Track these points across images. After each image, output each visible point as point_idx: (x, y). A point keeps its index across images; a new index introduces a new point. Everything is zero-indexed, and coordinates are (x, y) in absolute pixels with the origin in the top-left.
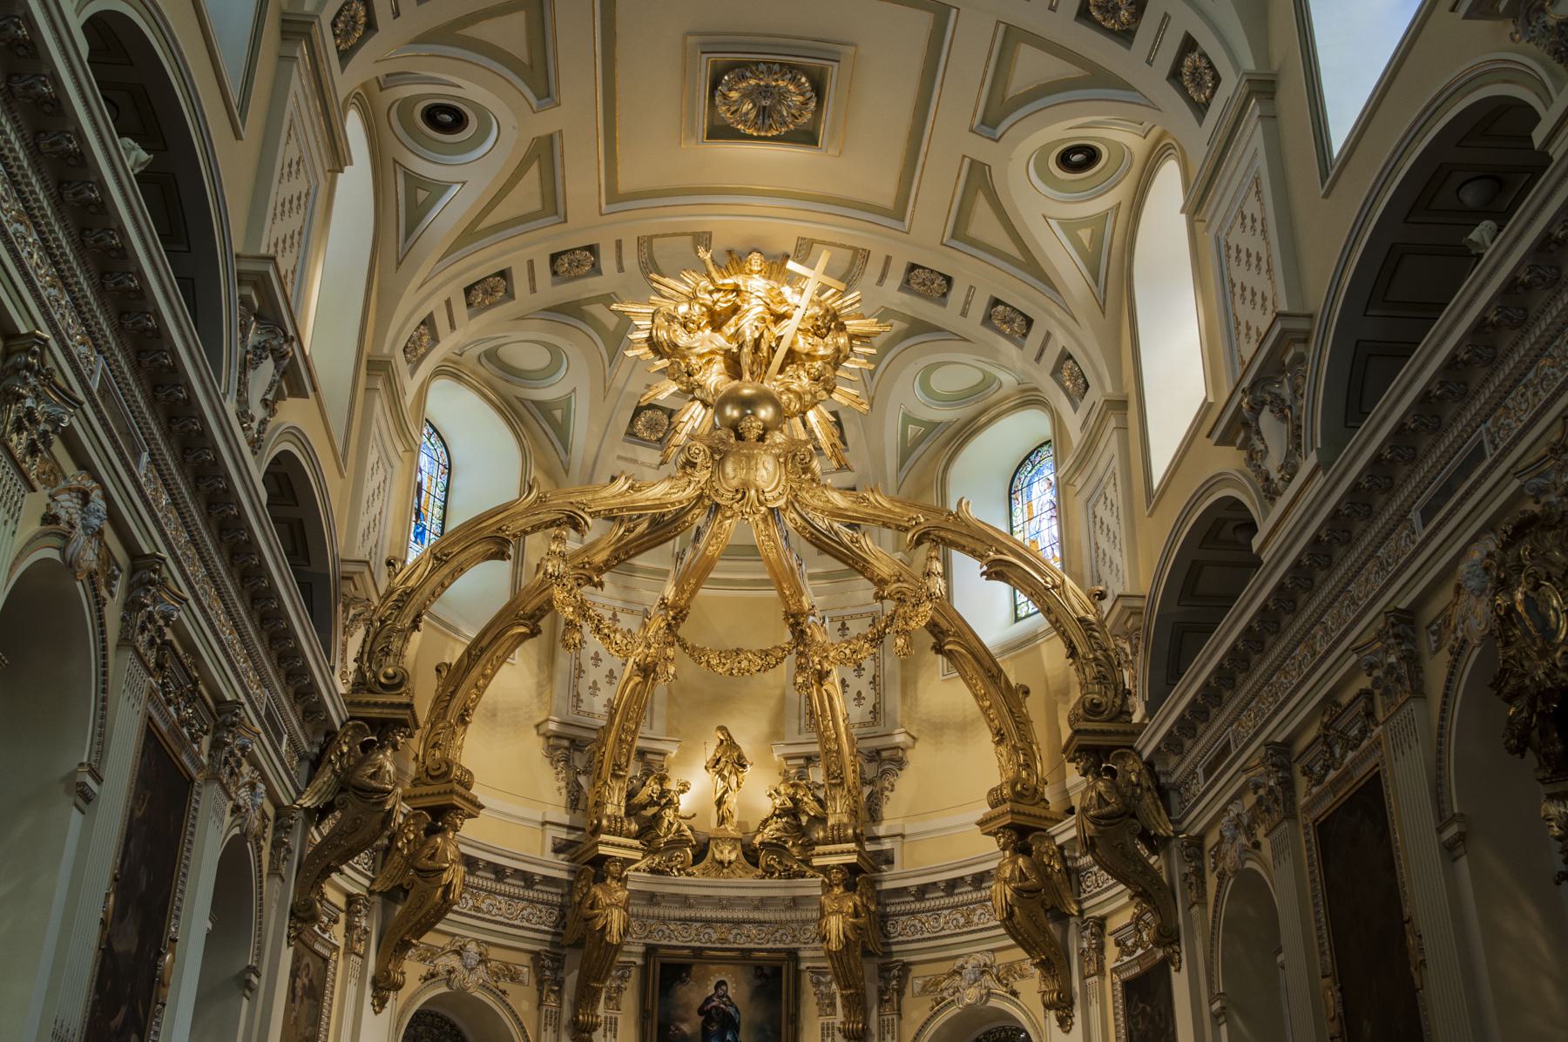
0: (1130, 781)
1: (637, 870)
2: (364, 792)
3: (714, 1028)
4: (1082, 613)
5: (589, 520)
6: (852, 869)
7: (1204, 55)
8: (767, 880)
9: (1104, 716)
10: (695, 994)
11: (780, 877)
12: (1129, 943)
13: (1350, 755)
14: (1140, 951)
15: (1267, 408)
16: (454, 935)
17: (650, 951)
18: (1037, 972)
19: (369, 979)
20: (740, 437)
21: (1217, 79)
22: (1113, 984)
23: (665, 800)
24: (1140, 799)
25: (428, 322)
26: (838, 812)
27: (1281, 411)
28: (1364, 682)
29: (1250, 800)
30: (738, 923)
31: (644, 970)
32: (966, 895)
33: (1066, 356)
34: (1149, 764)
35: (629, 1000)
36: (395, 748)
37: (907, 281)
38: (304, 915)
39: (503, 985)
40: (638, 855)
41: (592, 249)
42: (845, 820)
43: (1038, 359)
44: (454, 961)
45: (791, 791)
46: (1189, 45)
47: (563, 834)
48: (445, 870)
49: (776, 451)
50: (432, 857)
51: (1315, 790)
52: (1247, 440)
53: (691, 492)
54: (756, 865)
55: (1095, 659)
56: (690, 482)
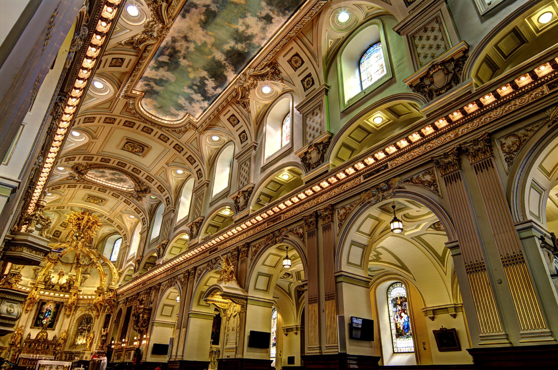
3: (47, 312)
6: (75, 293)
10: (46, 307)
23: (50, 279)
31: (39, 303)
40: (43, 288)
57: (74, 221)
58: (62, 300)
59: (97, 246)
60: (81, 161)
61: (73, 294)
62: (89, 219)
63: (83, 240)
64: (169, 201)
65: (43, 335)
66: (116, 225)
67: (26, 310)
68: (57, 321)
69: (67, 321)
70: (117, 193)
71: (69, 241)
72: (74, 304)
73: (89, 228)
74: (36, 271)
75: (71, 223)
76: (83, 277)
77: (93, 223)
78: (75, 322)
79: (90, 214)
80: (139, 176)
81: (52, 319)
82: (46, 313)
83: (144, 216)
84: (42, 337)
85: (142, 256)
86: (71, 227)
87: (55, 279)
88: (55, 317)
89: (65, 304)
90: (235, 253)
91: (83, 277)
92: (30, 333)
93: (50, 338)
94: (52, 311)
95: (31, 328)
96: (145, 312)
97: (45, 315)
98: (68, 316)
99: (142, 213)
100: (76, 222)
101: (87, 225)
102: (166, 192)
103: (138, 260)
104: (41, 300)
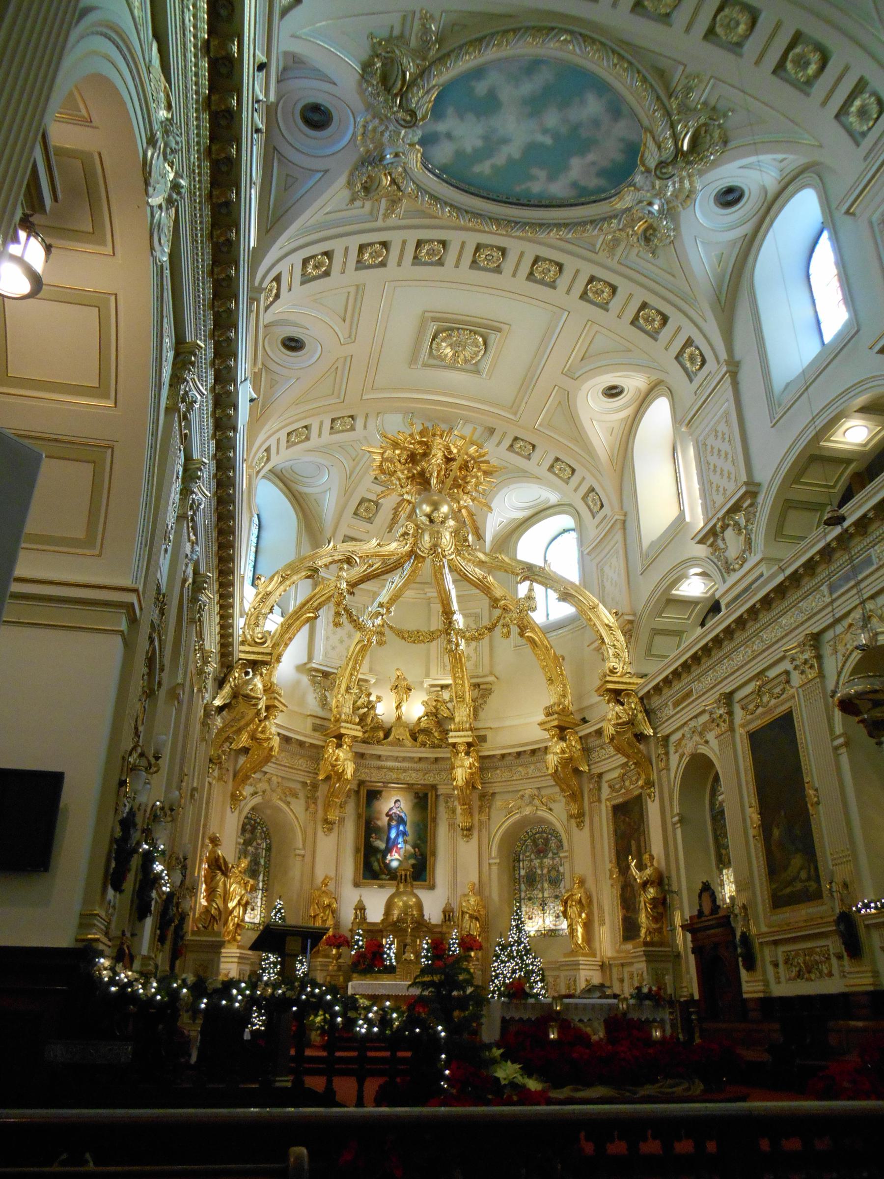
0: (631, 708)
1: (356, 741)
2: (247, 697)
3: (394, 823)
4: (607, 622)
5: (358, 560)
6: (469, 745)
7: (697, 348)
8: (423, 749)
9: (619, 674)
11: (430, 747)
12: (617, 787)
13: (773, 701)
14: (623, 791)
15: (730, 528)
16: (266, 773)
17: (361, 783)
18: (564, 800)
19: (229, 794)
20: (431, 521)
21: (704, 362)
22: (607, 807)
23: (371, 706)
24: (636, 716)
25: (268, 450)
26: (462, 714)
27: (740, 530)
28: (786, 665)
29: (705, 718)
30: (405, 770)
31: (357, 792)
32: (525, 759)
33: (592, 490)
34: (641, 699)
35: (350, 809)
36: (261, 675)
37: (511, 446)
39: (289, 799)
40: (360, 734)
41: (352, 417)
42: (465, 719)
43: (576, 490)
45: (434, 704)
46: (689, 342)
47: (318, 722)
48: (270, 739)
49: (451, 530)
50: (263, 732)
51: (749, 717)
52: (715, 541)
53: (407, 548)
54: (415, 739)
55: (614, 645)
56: (406, 544)
58: (430, 779)
61: (461, 748)
63: (451, 523)
67: (326, 821)
68: (434, 854)
69: (468, 850)
71: (405, 534)
72: (474, 787)
77: (465, 466)
78: (494, 853)
81: (414, 847)
82: (390, 827)
83: (689, 330)
87: (385, 710)
89: (442, 790)
90: (807, 655)
91: (477, 686)
92: (360, 901)
94: (408, 819)
95: (356, 885)
97: (389, 838)
98: (468, 831)
100: (409, 470)
104: (361, 783)
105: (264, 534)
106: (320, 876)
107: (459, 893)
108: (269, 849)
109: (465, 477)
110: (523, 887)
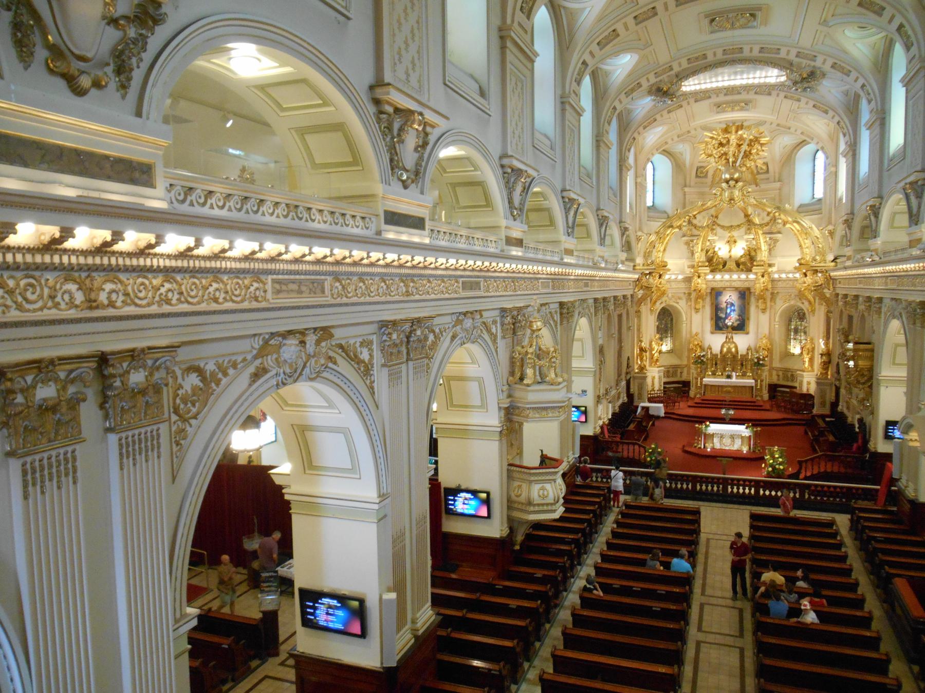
31: (711, 293)
35: (708, 299)
38: (638, 312)
44: (667, 298)
47: (690, 263)
57: (714, 152)
58: (746, 285)
59: (780, 174)
60: (653, 80)
61: (759, 274)
62: (741, 138)
63: (740, 184)
64: (869, 94)
65: (729, 350)
66: (799, 132)
68: (748, 319)
69: (764, 319)
70: (765, 90)
73: (747, 155)
74: (689, 245)
75: (710, 156)
76: (770, 239)
79: (740, 127)
80: (783, 54)
81: (739, 316)
82: (727, 308)
84: (729, 350)
85: (852, 213)
86: (714, 164)
87: (723, 250)
88: (744, 313)
89: (752, 290)
93: (742, 350)
95: (712, 333)
96: (860, 356)
98: (764, 311)
99: (831, 113)
101: (739, 152)
102: (854, 74)
103: (846, 221)
104: (712, 289)
105: (656, 173)
106: (694, 331)
107: (760, 336)
108: (672, 320)
109: (750, 151)
110: (792, 334)
